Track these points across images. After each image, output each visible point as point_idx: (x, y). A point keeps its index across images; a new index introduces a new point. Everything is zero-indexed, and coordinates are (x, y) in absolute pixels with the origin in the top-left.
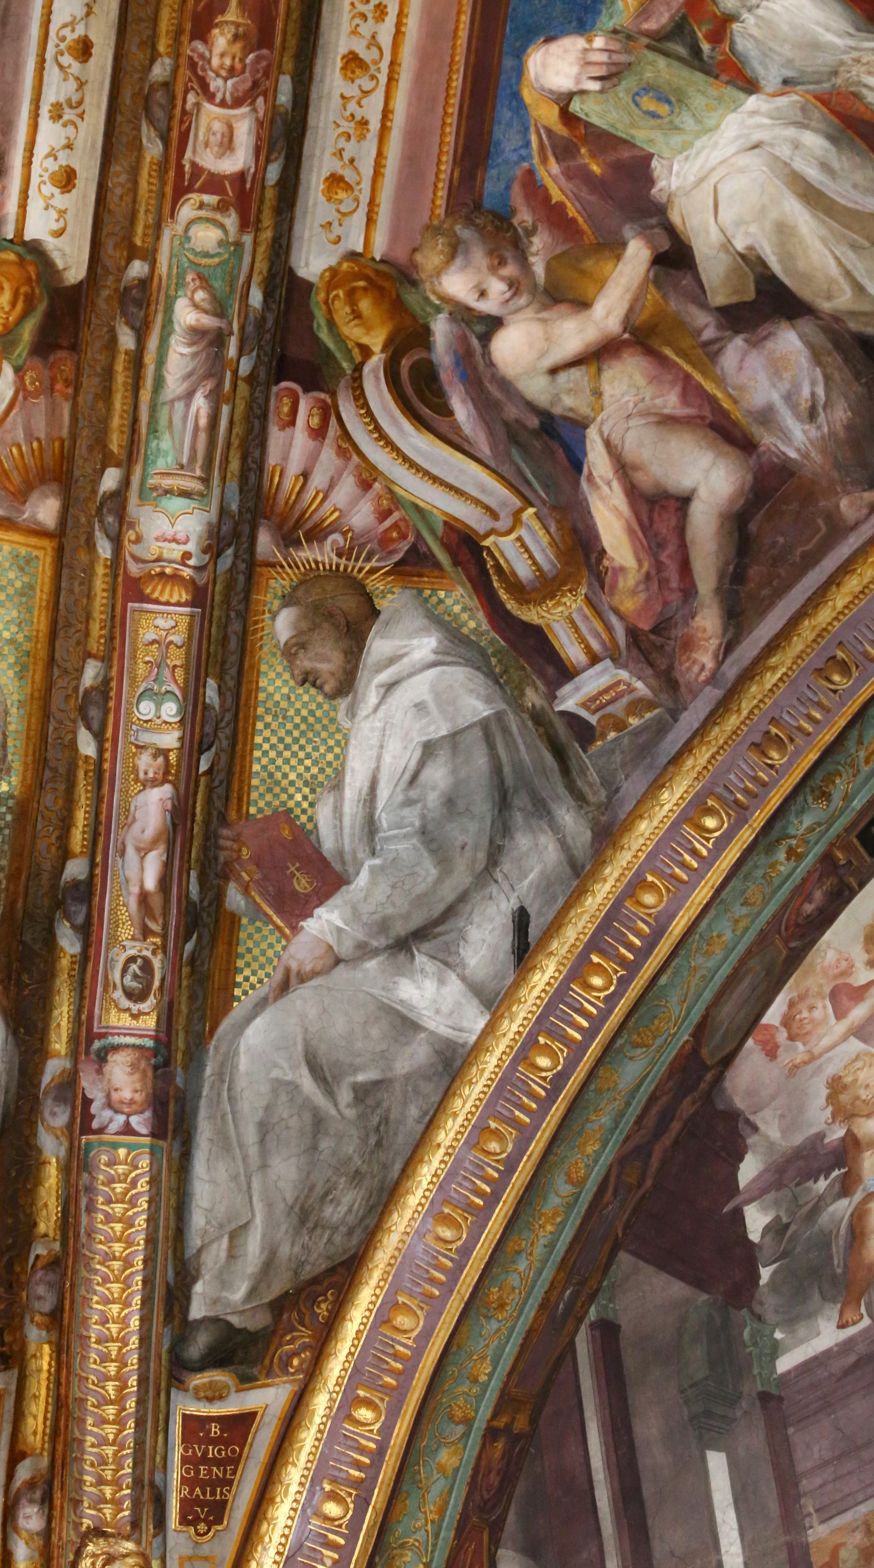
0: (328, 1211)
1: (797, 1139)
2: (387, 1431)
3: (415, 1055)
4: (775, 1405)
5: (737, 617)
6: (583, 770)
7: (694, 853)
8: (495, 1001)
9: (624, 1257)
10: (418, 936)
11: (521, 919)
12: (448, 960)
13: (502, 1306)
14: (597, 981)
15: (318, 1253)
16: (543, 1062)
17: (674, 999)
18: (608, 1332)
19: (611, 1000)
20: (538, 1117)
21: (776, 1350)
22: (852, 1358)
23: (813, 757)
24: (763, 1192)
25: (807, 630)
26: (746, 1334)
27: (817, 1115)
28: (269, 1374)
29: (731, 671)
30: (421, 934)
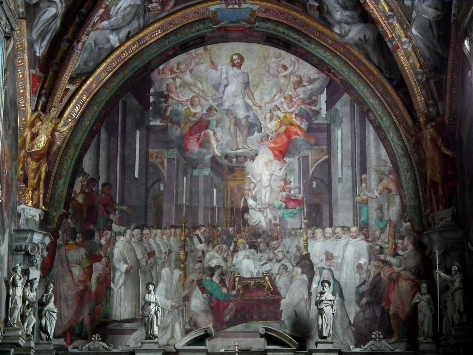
0: (89, 64)
1: (160, 90)
2: (86, 99)
3: (108, 46)
4: (149, 129)
5: (175, 5)
6: (146, 16)
7: (155, 34)
8: (122, 44)
9: (130, 93)
10: (115, 29)
11: (129, 33)
12: (118, 34)
13: (108, 89)
14: (135, 46)
15: (86, 69)
16: (124, 54)
17: (145, 55)
18: (125, 103)
19: (136, 49)
20: (121, 62)
21: (150, 121)
22: (161, 128)
23: (176, 28)
24: (154, 95)
25: (184, 11)
26: (146, 116)
27: (164, 88)
28: (73, 84)
29: (171, 11)
30: (116, 29)
